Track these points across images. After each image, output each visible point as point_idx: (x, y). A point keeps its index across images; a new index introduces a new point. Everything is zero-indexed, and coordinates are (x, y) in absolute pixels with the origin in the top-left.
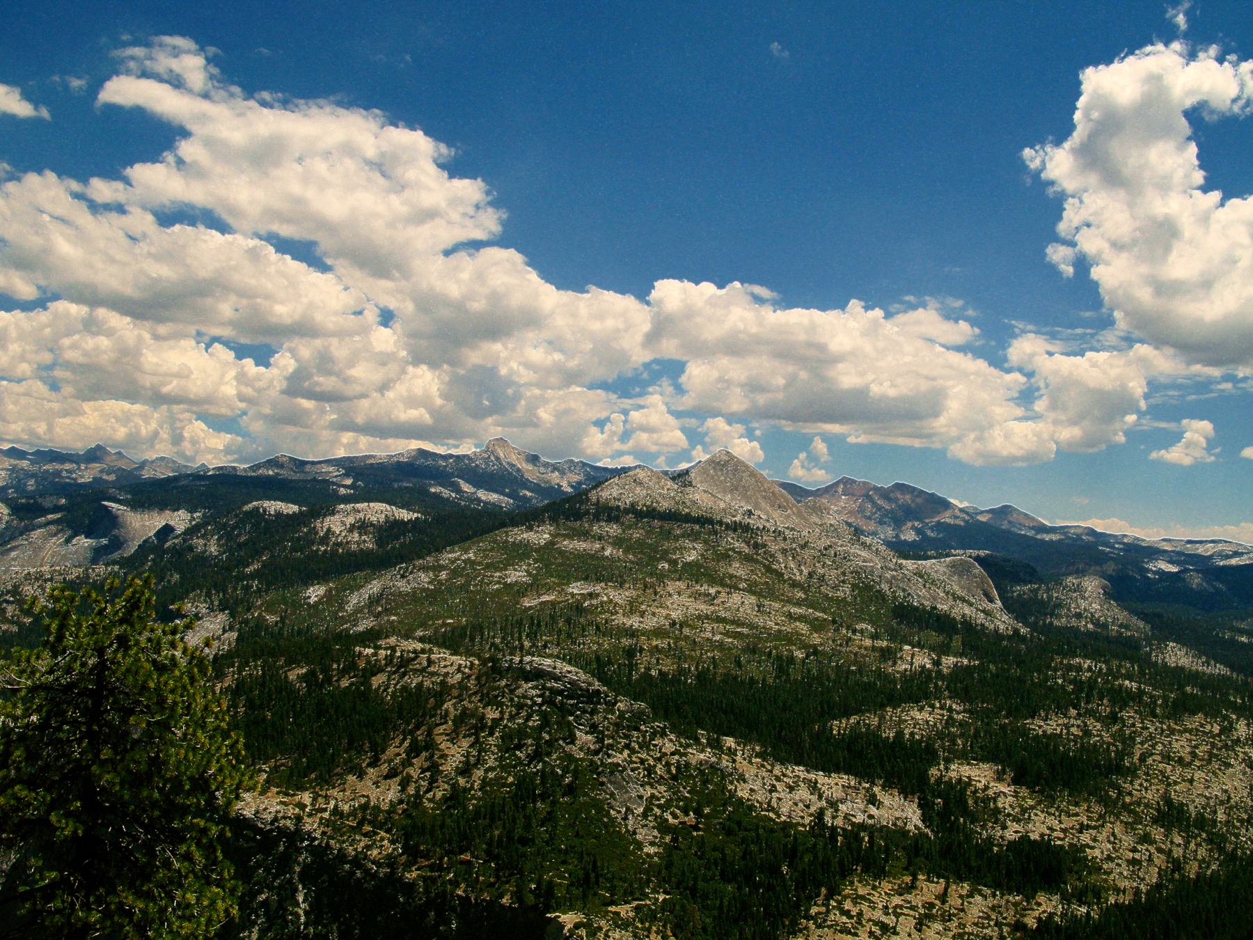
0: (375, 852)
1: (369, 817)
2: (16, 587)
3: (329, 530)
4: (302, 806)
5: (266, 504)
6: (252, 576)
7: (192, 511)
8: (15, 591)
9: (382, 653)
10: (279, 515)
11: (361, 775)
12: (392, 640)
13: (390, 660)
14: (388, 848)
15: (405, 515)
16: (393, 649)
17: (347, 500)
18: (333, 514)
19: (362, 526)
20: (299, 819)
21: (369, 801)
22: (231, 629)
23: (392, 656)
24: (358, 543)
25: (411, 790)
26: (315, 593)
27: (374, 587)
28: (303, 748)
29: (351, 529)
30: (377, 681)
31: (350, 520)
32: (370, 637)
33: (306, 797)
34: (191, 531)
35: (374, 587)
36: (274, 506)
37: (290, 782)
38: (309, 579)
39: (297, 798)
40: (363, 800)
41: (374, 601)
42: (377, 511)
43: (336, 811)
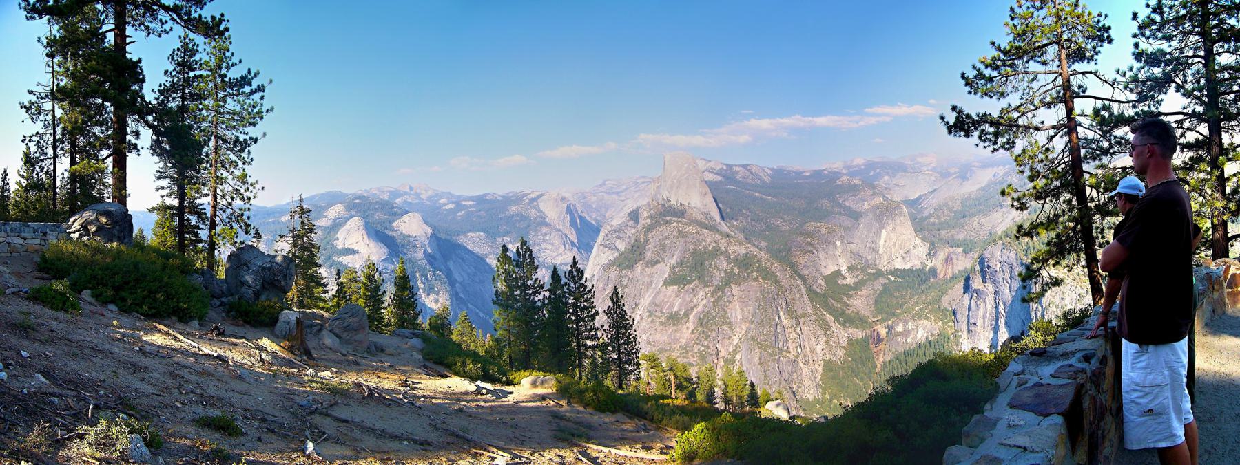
8: (946, 205)
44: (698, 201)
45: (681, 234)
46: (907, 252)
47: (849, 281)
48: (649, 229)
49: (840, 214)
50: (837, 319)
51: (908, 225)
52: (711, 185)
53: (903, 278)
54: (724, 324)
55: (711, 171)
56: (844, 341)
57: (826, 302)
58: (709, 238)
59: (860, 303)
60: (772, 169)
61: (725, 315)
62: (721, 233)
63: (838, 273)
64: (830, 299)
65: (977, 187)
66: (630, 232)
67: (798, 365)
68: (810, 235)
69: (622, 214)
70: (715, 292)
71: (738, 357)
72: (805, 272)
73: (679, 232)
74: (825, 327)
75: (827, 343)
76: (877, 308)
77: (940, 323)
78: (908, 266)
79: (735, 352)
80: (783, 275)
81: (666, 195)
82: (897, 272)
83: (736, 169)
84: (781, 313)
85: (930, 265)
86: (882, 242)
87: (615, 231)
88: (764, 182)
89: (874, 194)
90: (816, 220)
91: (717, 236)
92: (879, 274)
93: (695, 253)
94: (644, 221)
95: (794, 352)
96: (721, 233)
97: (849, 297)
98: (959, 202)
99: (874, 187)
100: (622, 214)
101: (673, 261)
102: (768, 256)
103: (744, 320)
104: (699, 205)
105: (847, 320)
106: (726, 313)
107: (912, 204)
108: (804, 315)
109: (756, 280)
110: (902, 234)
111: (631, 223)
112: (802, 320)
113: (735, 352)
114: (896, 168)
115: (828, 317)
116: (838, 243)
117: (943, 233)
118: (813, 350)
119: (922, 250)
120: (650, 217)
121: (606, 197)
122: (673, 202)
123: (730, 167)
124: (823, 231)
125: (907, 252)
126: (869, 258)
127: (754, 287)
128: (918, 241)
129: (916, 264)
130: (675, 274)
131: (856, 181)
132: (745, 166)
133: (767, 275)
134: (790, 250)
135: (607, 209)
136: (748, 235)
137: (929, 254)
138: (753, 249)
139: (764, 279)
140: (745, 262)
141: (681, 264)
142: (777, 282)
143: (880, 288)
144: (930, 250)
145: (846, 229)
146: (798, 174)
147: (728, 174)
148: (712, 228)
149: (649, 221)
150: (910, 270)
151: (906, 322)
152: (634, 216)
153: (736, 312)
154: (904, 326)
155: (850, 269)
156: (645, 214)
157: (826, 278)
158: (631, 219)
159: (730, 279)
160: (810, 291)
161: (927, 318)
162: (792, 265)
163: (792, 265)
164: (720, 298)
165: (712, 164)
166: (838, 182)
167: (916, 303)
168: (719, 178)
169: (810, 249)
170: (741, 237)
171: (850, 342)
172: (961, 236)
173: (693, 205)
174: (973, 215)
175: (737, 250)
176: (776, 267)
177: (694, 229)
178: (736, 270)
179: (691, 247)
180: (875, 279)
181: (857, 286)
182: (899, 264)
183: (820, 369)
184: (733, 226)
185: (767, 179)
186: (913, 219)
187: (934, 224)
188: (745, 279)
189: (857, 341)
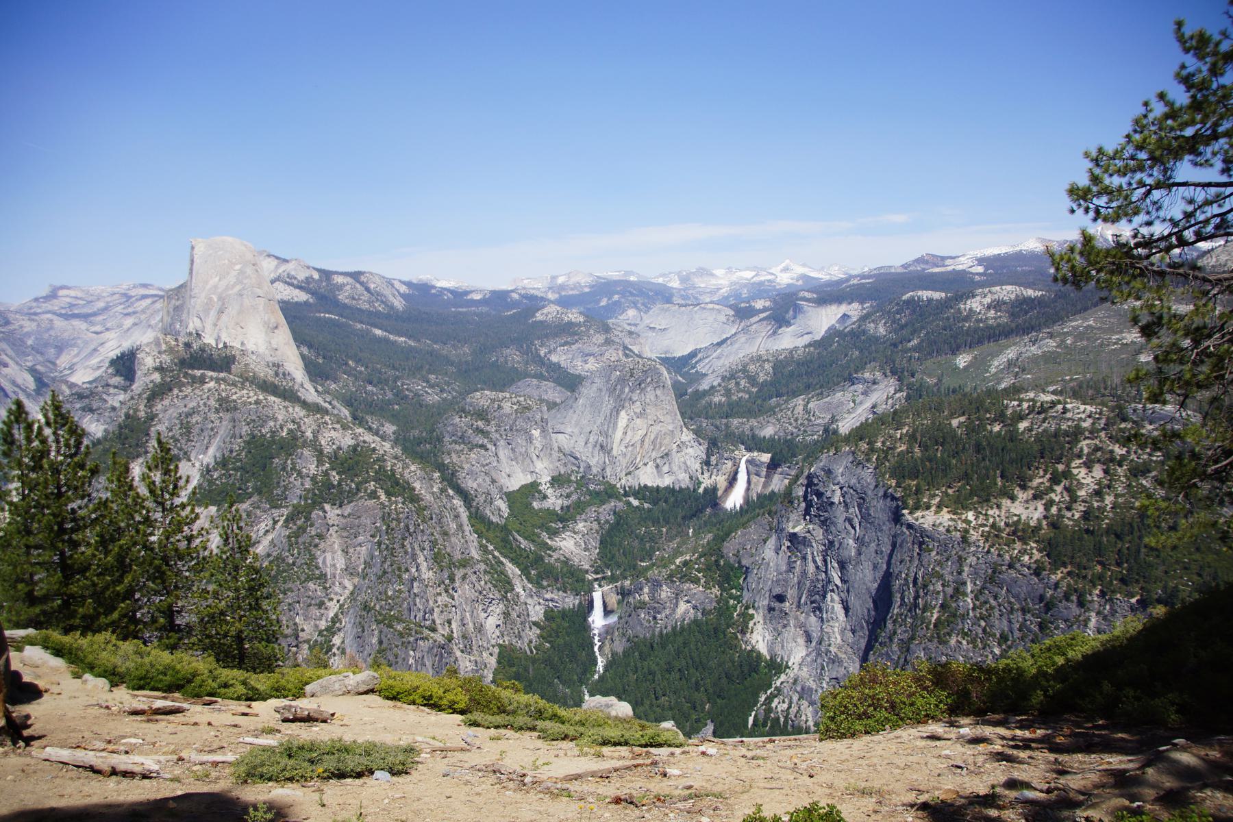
0: (1026, 558)
1: (1020, 532)
2: (745, 366)
3: (971, 309)
4: (968, 522)
5: (920, 293)
6: (915, 349)
7: (862, 303)
8: (744, 370)
9: (1025, 405)
10: (930, 300)
11: (1013, 498)
12: (1031, 395)
13: (1031, 410)
14: (1037, 555)
15: (1030, 293)
16: (1032, 400)
17: (982, 285)
18: (973, 297)
19: (997, 305)
20: (967, 531)
21: (1019, 520)
22: (900, 390)
23: (1034, 406)
24: (995, 318)
25: (1054, 510)
26: (962, 360)
27: (1011, 353)
28: (966, 476)
29: (989, 307)
30: (1023, 425)
31: (988, 300)
32: (1014, 391)
33: (970, 515)
34: (864, 318)
35: (1011, 353)
36: (925, 294)
37: (958, 504)
38: (955, 350)
39: (963, 517)
40: (1015, 518)
41: (1010, 364)
42: (1008, 292)
43: (993, 526)
44: (264, 341)
45: (226, 405)
46: (667, 455)
47: (554, 501)
48: (157, 393)
49: (540, 377)
50: (525, 571)
51: (669, 402)
52: (291, 311)
53: (655, 502)
54: (309, 578)
55: (289, 281)
56: (537, 612)
57: (505, 541)
58: (281, 413)
59: (573, 545)
60: (408, 284)
61: (311, 562)
62: (305, 404)
63: (532, 489)
64: (518, 533)
65: (807, 339)
66: (117, 399)
67: (450, 653)
68: (482, 414)
69: (94, 361)
70: (290, 519)
71: (337, 640)
72: (470, 484)
73: (221, 401)
74: (505, 585)
75: (506, 615)
76: (602, 555)
77: (716, 590)
78: (666, 481)
79: (331, 630)
80: (425, 485)
81: (193, 324)
82: (642, 492)
83: (339, 280)
84: (421, 559)
85: (706, 482)
86: (619, 434)
87: (81, 396)
88: (392, 307)
89: (608, 342)
90: (493, 388)
91: (299, 412)
92: (609, 493)
93: (253, 442)
94: (146, 377)
95: (443, 630)
96: (305, 404)
97: (554, 533)
98: (768, 366)
99: (607, 329)
100: (94, 361)
101: (208, 458)
102: (398, 451)
103: (349, 571)
104: (262, 349)
105: (543, 571)
106: (313, 557)
107: (680, 364)
108: (465, 563)
109: (373, 495)
110: (657, 421)
111: (117, 380)
112: (459, 573)
113: (331, 630)
114: (651, 295)
115: (511, 569)
116: (536, 433)
117: (735, 422)
118: (480, 629)
119: (693, 453)
120: (160, 369)
121: (59, 323)
122: (209, 340)
123: (326, 274)
124: (507, 407)
125: (667, 455)
126: (593, 462)
127: (372, 506)
128: (687, 436)
129: (684, 480)
130: (211, 482)
131: (574, 316)
132: (356, 276)
133: (397, 486)
134: (440, 439)
135: (60, 349)
136: (360, 409)
137: (707, 463)
138: (368, 437)
139: (388, 494)
140: (353, 463)
141: (223, 463)
142: (414, 499)
143: (612, 518)
144: (709, 454)
145: (552, 406)
146: (459, 296)
147: (322, 289)
148: (290, 395)
149: (157, 377)
150: (670, 490)
151: (656, 585)
152: (125, 365)
153: (332, 558)
154: (653, 591)
155: (557, 481)
156: (149, 362)
157: (510, 497)
158: (118, 373)
159: (324, 493)
160: (478, 518)
161: (696, 581)
162: (441, 467)
163: (441, 467)
164: (302, 530)
165: (290, 268)
166: (539, 316)
167: (677, 553)
168: (301, 296)
169: (480, 440)
170: (345, 412)
171: (549, 615)
172: (768, 431)
173: (250, 346)
174: (795, 394)
175: (337, 438)
176: (412, 472)
177: (248, 395)
178: (335, 477)
179: (245, 429)
180: (603, 502)
181: (565, 518)
182: (648, 477)
183: (493, 662)
184: (328, 392)
185: (399, 304)
186: (679, 391)
187: (720, 404)
188: (352, 495)
189: (564, 614)
